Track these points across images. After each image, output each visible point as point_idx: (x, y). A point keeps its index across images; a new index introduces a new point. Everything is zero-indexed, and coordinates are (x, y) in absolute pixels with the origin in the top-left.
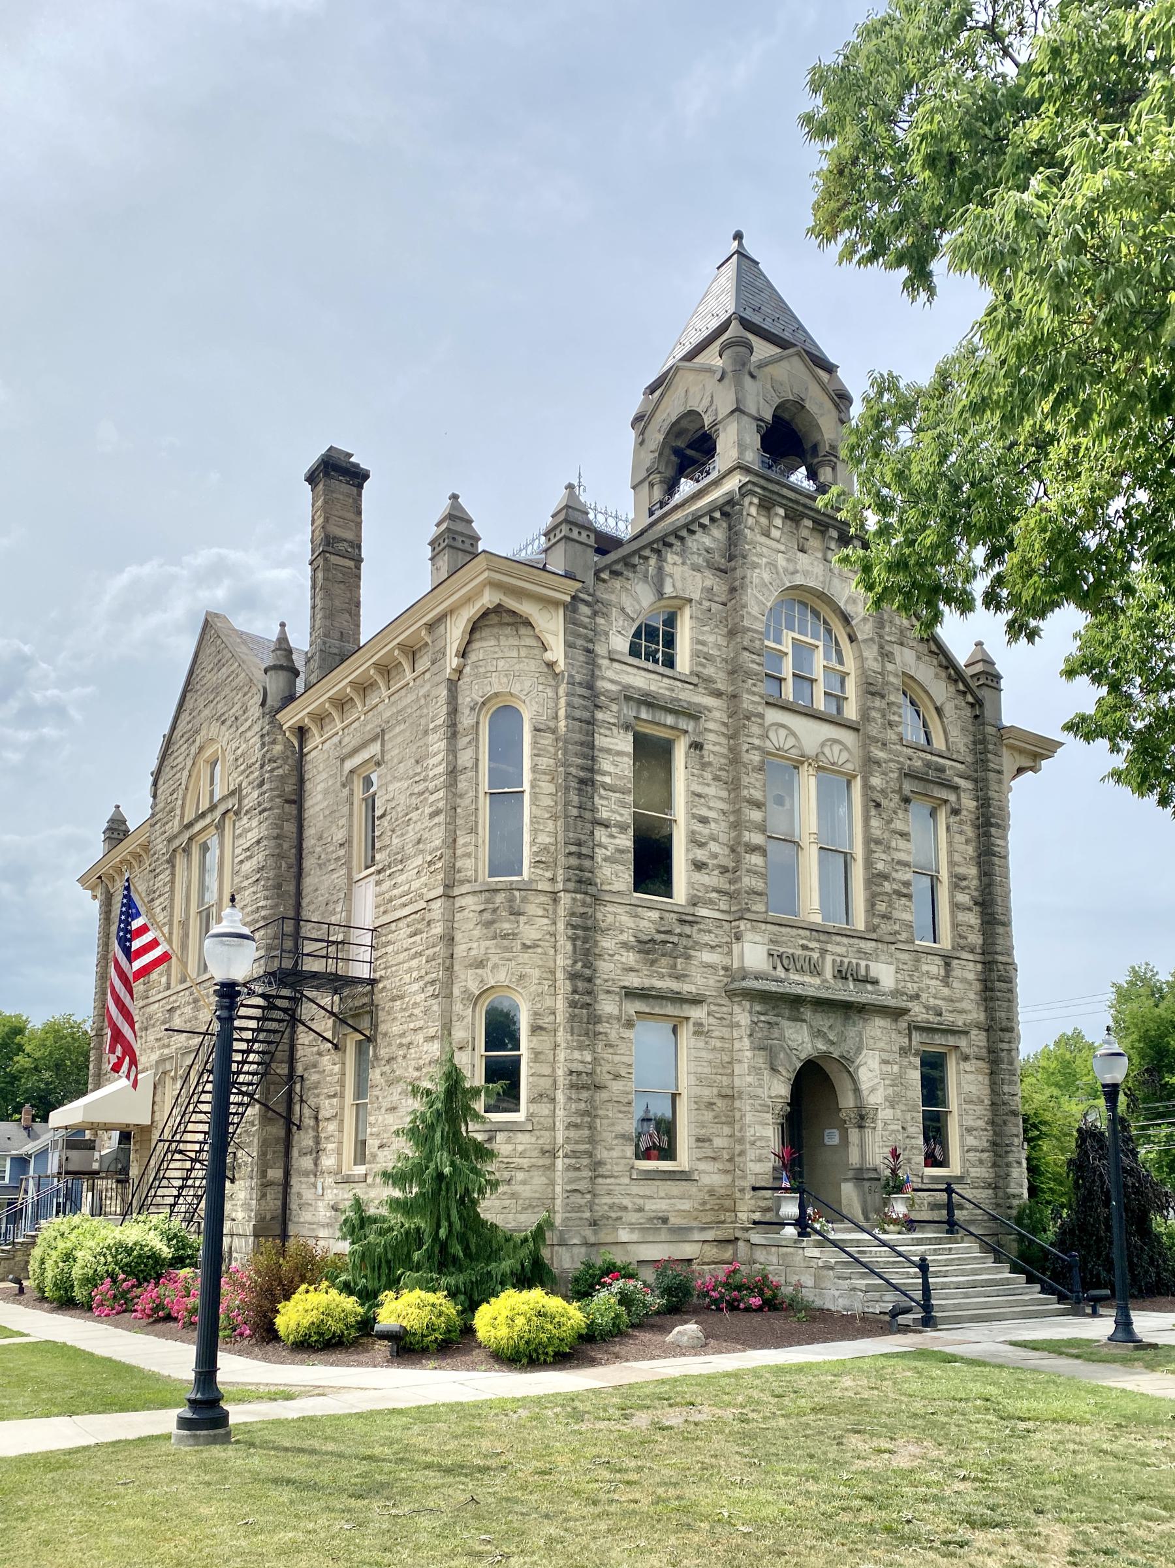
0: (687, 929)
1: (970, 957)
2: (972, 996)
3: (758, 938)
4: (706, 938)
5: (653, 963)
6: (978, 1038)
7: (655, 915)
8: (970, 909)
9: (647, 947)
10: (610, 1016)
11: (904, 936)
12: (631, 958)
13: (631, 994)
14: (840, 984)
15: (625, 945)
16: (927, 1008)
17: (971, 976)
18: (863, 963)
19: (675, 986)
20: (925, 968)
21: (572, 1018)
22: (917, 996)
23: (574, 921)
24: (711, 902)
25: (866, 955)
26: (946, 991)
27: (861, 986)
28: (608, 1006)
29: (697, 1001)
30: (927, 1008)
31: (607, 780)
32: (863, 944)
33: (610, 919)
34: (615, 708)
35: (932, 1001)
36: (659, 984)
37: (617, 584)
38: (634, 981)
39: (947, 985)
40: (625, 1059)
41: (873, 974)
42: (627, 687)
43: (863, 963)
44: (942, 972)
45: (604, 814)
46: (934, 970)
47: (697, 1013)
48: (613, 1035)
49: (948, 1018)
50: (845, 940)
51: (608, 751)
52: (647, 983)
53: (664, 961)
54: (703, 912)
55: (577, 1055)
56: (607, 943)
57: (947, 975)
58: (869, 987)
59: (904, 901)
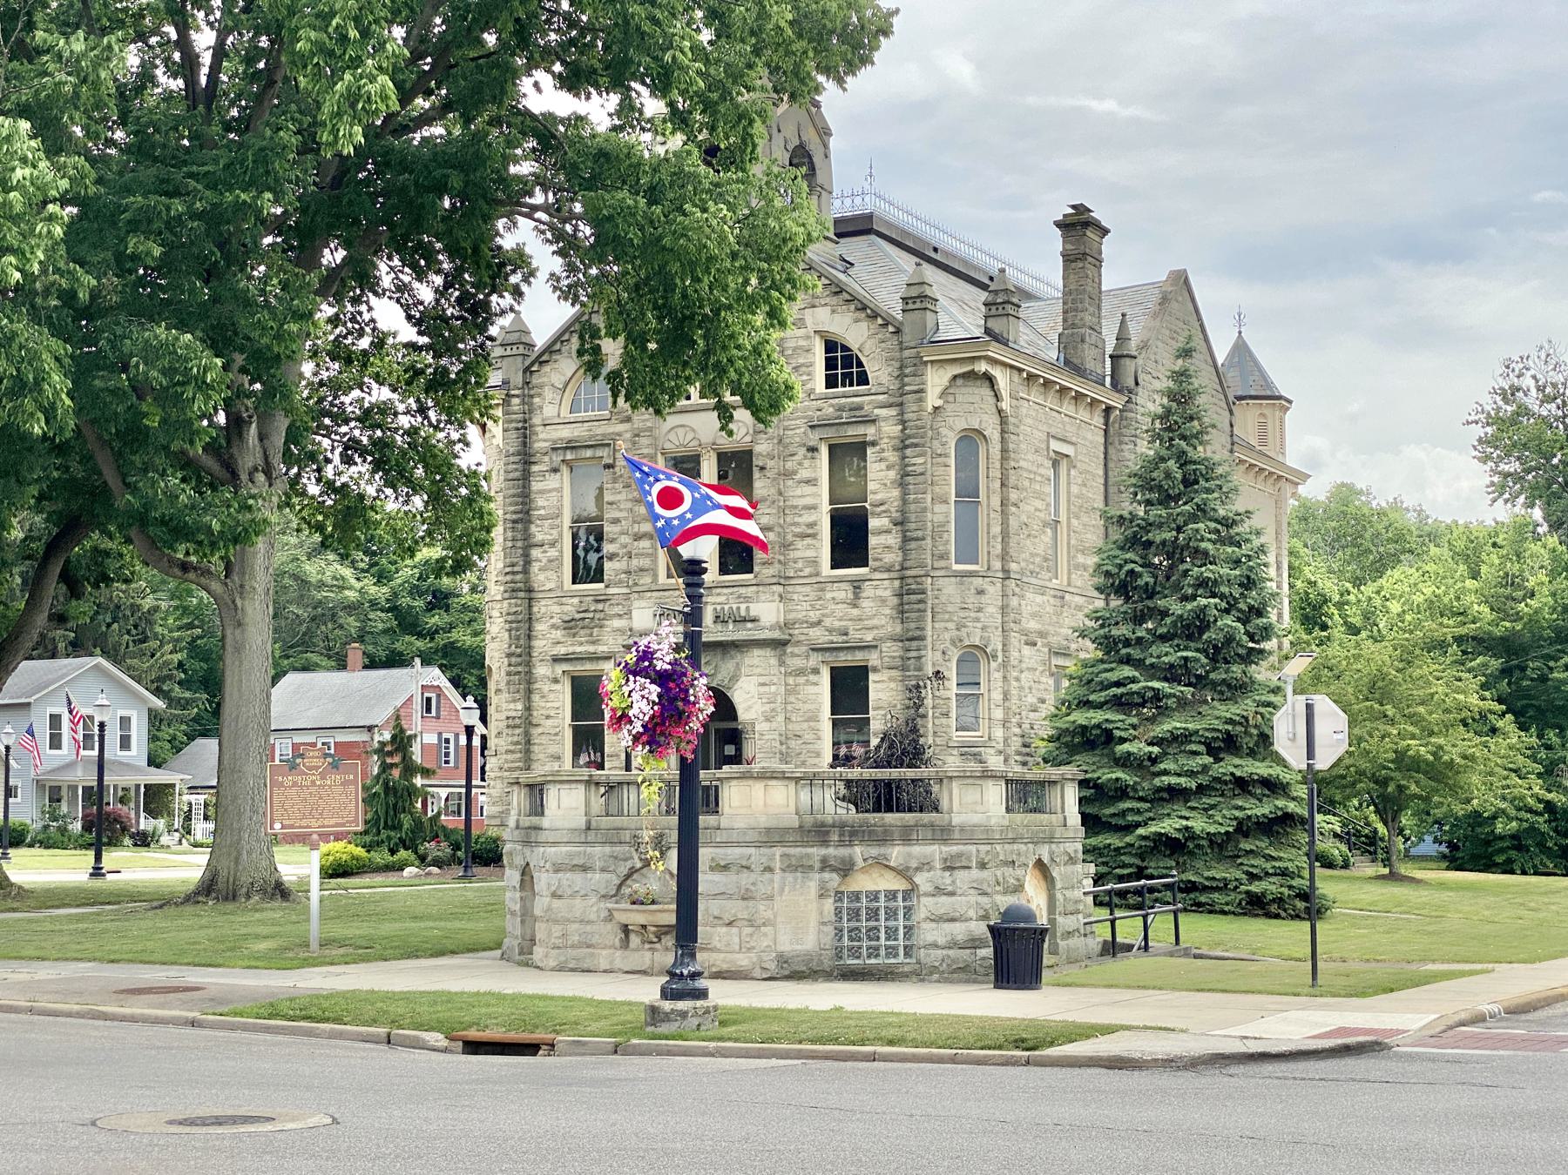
0: (600, 606)
1: (885, 576)
2: (888, 611)
3: (643, 603)
4: (617, 610)
5: (574, 635)
6: (891, 650)
7: (576, 600)
8: (888, 532)
9: (570, 625)
10: (545, 676)
11: (807, 571)
12: (558, 634)
13: (556, 660)
14: (719, 627)
15: (553, 626)
16: (830, 631)
17: (888, 593)
18: (743, 607)
19: (591, 649)
20: (829, 595)
21: (508, 683)
22: (819, 623)
23: (510, 618)
24: (621, 582)
25: (747, 599)
26: (855, 612)
27: (740, 625)
28: (541, 670)
29: (608, 658)
30: (830, 631)
31: (542, 512)
32: (742, 590)
33: (543, 610)
34: (546, 459)
35: (837, 624)
36: (579, 649)
37: (547, 368)
38: (561, 650)
39: (855, 606)
40: (556, 705)
41: (753, 613)
42: (555, 442)
43: (743, 607)
44: (851, 596)
45: (539, 537)
46: (841, 595)
47: (608, 666)
48: (546, 688)
49: (855, 636)
50: (725, 591)
51: (541, 492)
52: (571, 649)
53: (582, 632)
54: (611, 591)
55: (512, 706)
56: (540, 627)
57: (857, 596)
58: (749, 625)
59: (809, 541)
